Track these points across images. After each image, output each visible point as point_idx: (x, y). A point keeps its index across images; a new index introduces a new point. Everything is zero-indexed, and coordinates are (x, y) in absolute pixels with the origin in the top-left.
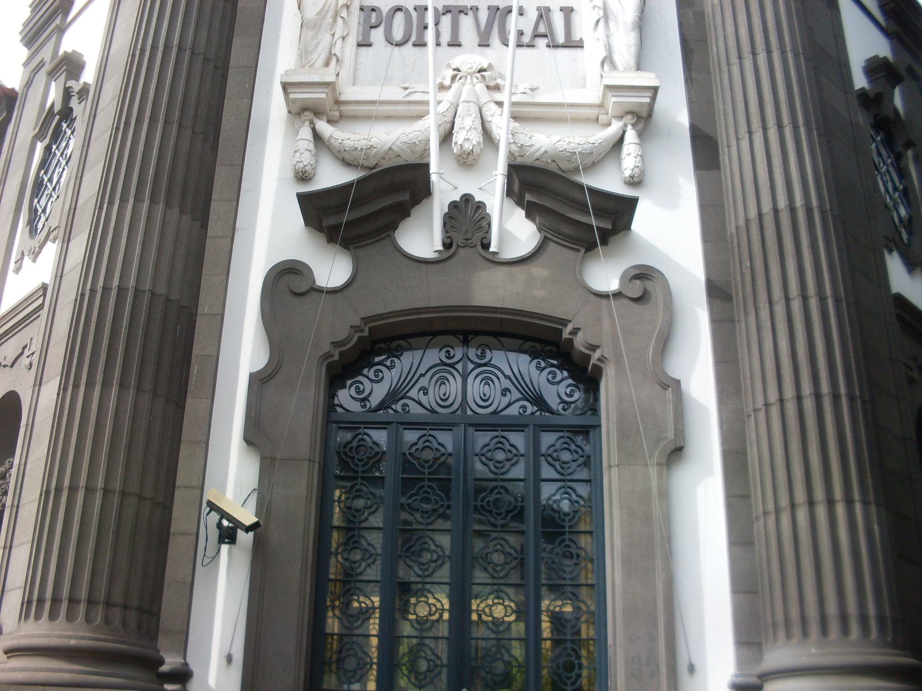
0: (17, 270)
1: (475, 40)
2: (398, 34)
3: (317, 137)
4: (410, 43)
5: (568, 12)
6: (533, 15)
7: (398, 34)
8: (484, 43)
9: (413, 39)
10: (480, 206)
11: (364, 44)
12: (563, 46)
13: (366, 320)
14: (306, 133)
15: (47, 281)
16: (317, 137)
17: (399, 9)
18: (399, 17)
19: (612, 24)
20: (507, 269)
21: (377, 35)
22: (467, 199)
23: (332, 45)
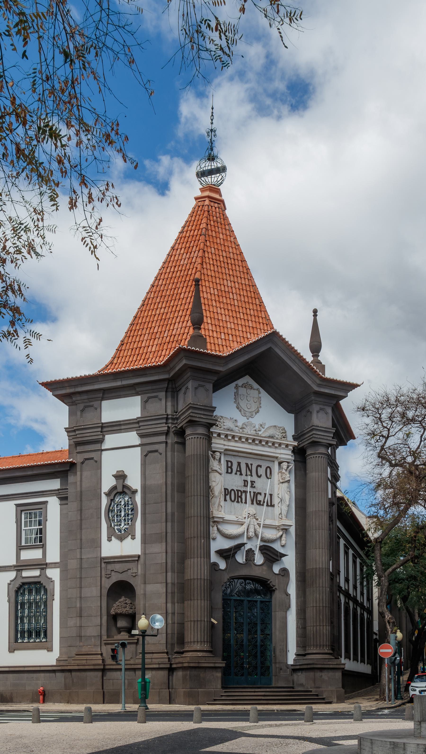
0: (109, 540)
1: (250, 502)
2: (233, 498)
3: (218, 529)
4: (235, 502)
5: (271, 495)
6: (263, 495)
7: (233, 498)
8: (252, 503)
9: (236, 500)
10: (254, 551)
11: (225, 500)
12: (270, 506)
13: (230, 577)
14: (215, 528)
15: (140, 554)
16: (218, 529)
17: (233, 490)
18: (233, 492)
19: (283, 502)
20: (258, 567)
21: (228, 497)
22: (251, 549)
23: (220, 502)
